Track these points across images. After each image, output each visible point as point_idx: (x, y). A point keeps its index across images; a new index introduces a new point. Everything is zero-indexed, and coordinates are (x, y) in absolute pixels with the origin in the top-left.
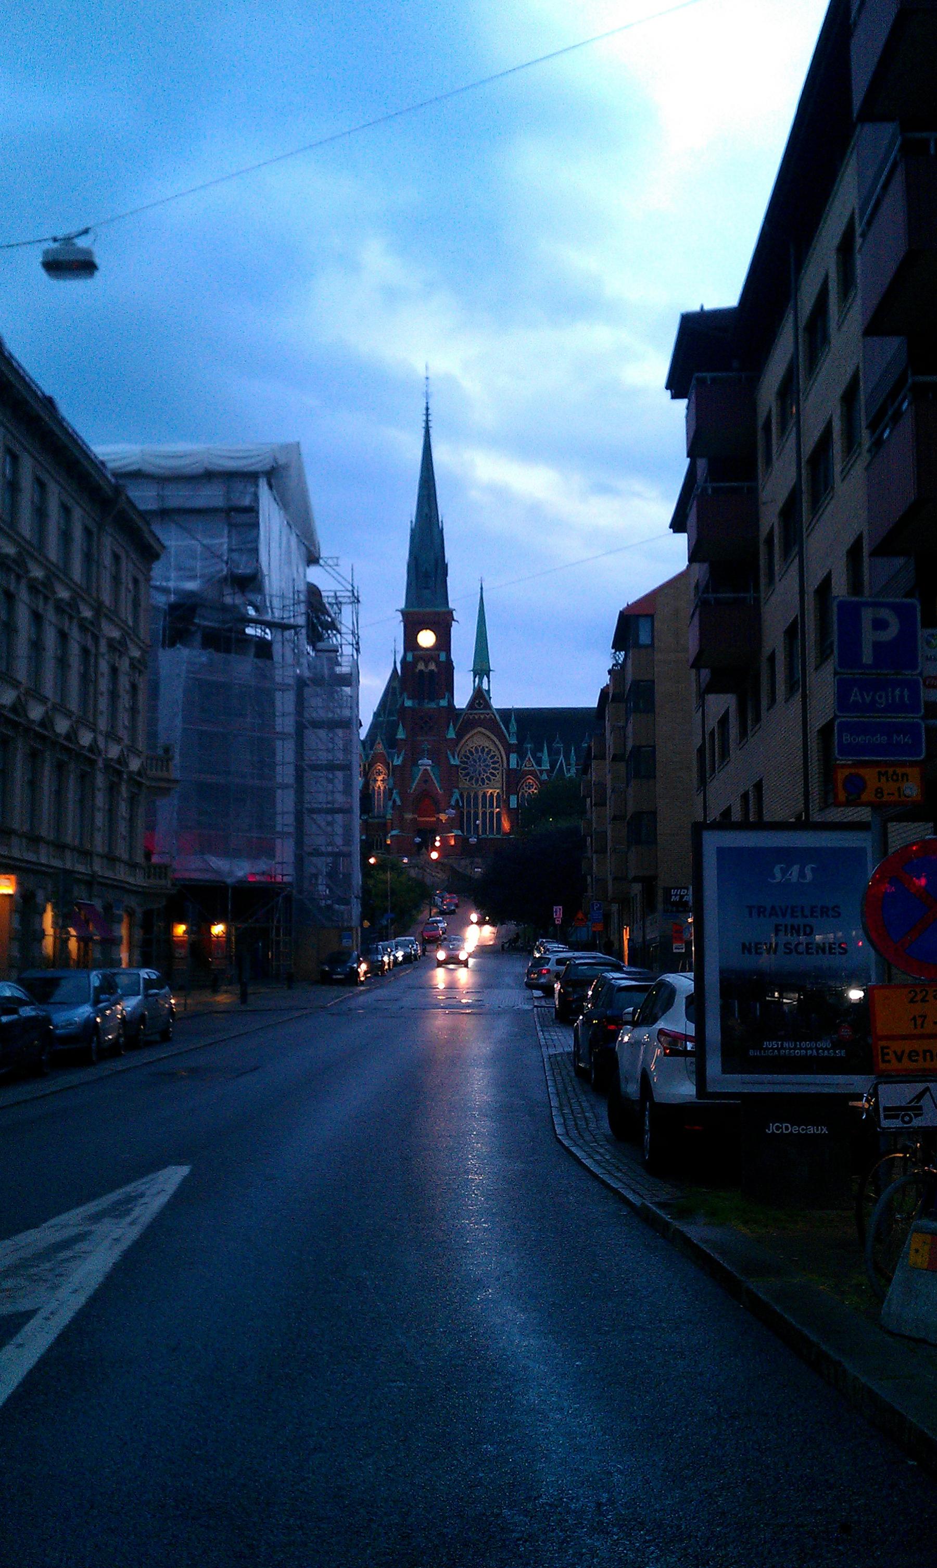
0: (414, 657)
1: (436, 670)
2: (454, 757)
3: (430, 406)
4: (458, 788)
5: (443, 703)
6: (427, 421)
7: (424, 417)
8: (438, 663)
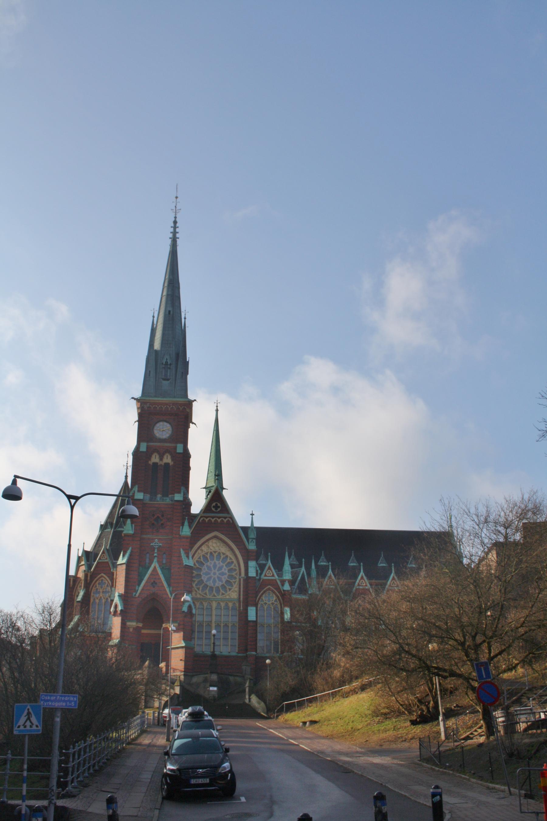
0: (148, 447)
3: (177, 220)
5: (178, 497)
6: (175, 233)
7: (172, 230)
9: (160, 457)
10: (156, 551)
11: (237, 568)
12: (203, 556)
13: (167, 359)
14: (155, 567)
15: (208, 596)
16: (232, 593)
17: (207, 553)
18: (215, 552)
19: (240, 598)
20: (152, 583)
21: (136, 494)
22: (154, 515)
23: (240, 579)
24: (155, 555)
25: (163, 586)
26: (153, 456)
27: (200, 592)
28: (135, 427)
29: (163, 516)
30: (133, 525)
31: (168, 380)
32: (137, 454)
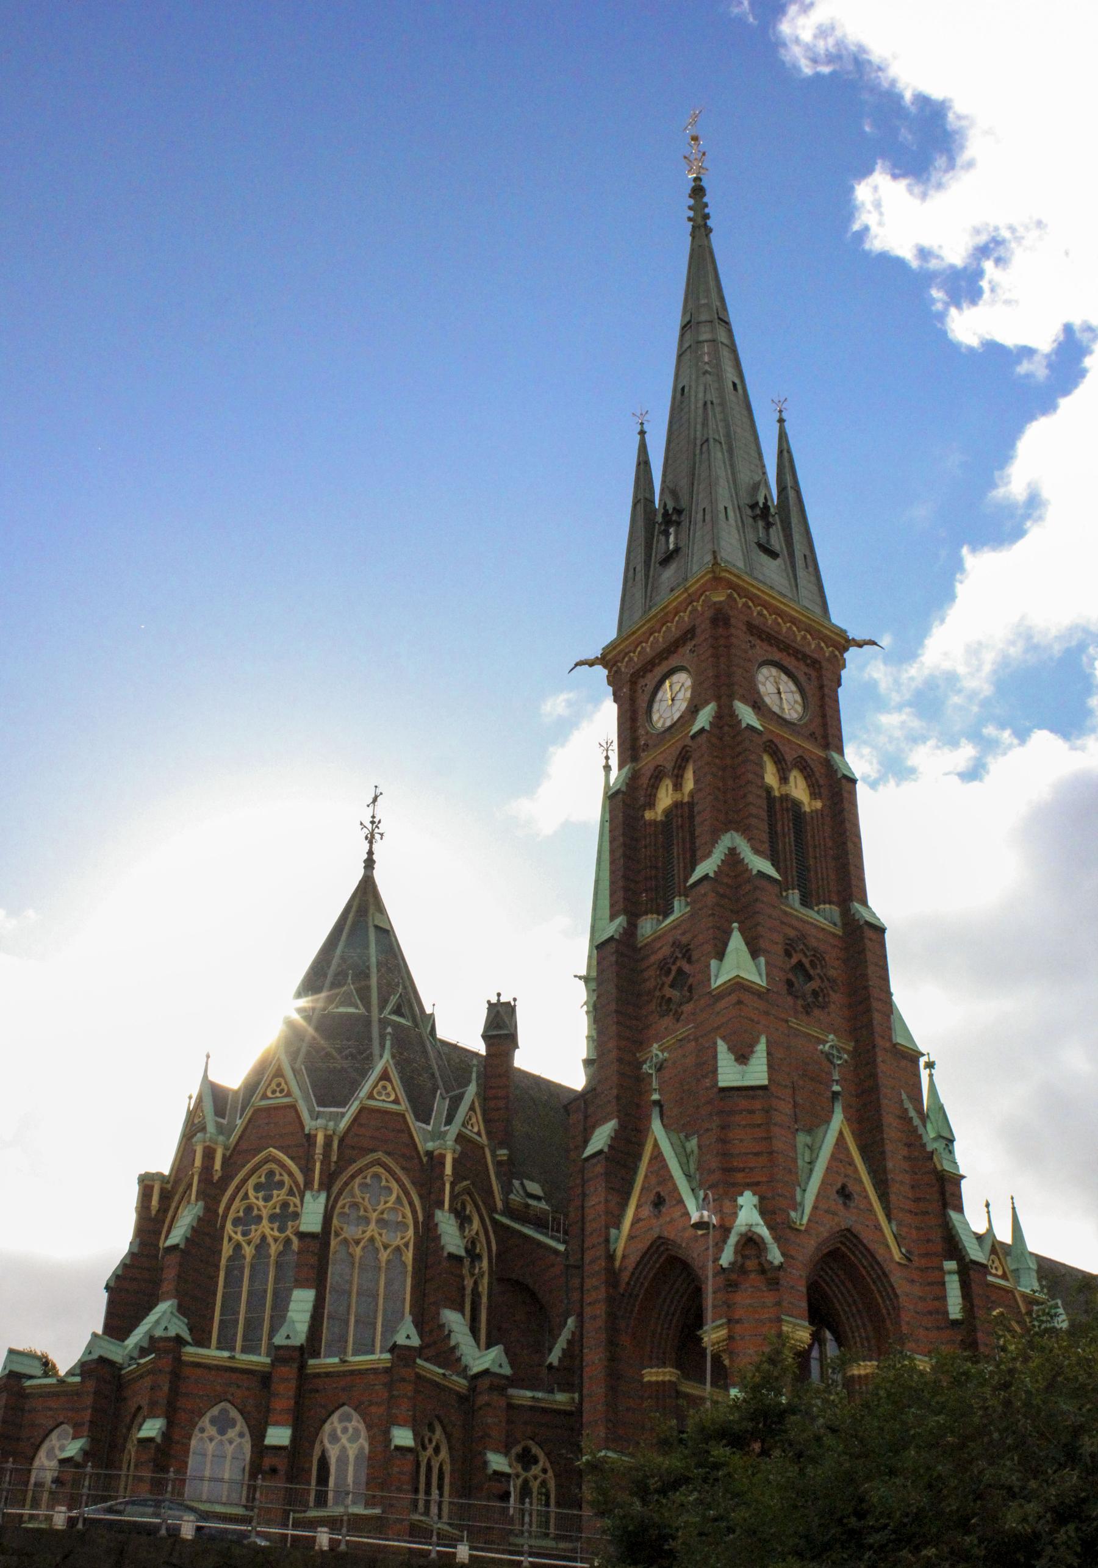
30: (762, 960)
31: (773, 555)
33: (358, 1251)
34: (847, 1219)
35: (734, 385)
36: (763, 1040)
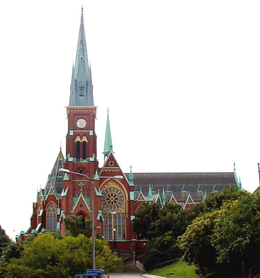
0: (74, 132)
1: (87, 141)
2: (98, 191)
4: (102, 209)
5: (92, 159)
6: (82, 14)
8: (88, 137)
9: (81, 138)
10: (81, 189)
11: (124, 196)
12: (106, 190)
13: (82, 85)
14: (81, 197)
15: (110, 211)
16: (122, 209)
17: (107, 188)
18: (112, 188)
19: (126, 212)
20: (80, 206)
21: (69, 159)
22: (79, 170)
23: (126, 201)
24: (81, 190)
25: (86, 206)
26: (77, 138)
27: (105, 209)
28: (67, 121)
29: (84, 170)
30: (69, 175)
31: (83, 96)
32: (68, 137)
33: (50, 215)
34: (81, 209)
35: (82, 58)
36: (68, 187)
